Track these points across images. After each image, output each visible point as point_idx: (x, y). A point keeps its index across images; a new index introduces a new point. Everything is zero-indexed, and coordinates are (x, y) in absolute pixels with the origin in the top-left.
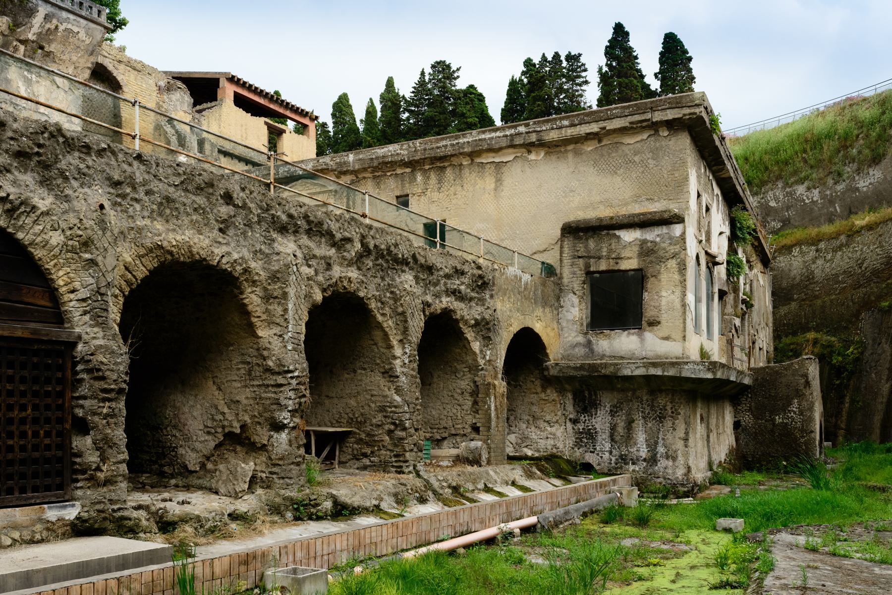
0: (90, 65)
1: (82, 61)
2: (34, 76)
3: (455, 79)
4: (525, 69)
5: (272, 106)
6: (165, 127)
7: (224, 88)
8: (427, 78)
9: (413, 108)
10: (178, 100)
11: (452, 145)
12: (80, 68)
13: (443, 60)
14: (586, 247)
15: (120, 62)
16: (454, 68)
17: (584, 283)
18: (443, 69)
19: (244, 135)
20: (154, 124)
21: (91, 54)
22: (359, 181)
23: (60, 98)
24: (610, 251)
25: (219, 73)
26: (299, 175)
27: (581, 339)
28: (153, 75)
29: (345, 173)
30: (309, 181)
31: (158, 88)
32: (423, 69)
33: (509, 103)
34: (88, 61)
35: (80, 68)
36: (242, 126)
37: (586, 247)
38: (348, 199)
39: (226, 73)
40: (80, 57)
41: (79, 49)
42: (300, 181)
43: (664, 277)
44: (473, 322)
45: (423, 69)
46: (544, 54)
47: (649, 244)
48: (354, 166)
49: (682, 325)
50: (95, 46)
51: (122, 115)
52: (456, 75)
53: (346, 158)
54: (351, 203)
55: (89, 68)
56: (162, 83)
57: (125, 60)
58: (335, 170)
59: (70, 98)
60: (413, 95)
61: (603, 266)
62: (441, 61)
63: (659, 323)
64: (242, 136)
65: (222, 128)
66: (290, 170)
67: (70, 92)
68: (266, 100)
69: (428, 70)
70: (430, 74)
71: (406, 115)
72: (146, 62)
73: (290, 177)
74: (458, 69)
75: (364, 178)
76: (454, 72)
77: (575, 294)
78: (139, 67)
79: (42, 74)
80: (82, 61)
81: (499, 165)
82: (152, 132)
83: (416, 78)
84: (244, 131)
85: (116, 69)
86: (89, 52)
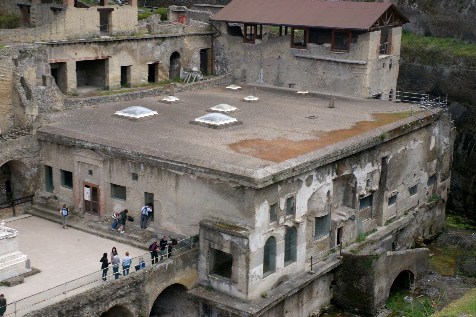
10: (27, 62)
11: (155, 161)
14: (209, 235)
17: (208, 252)
19: (83, 26)
24: (219, 241)
27: (206, 278)
36: (81, 19)
37: (209, 235)
43: (240, 262)
44: (131, 302)
47: (234, 244)
49: (246, 287)
61: (216, 247)
63: (237, 283)
77: (204, 256)
81: (177, 176)
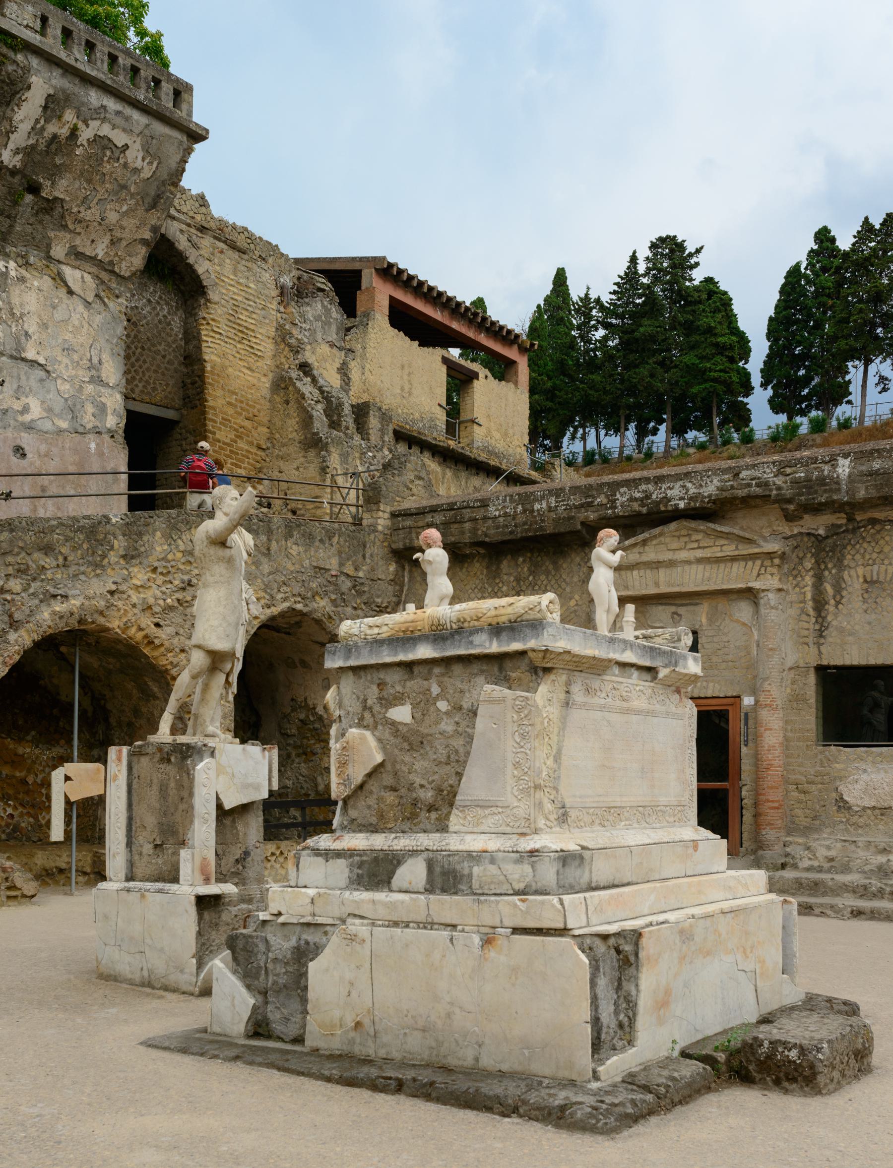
0: (147, 235)
1: (130, 223)
2: (12, 264)
3: (692, 267)
4: (816, 247)
5: (455, 325)
6: (298, 384)
7: (371, 290)
8: (642, 268)
9: (614, 321)
12: (124, 243)
13: (672, 234)
15: (202, 229)
16: (690, 248)
18: (672, 251)
20: (271, 375)
21: (154, 205)
22: (854, 531)
23: (75, 320)
25: (361, 259)
26: (676, 509)
28: (271, 260)
29: (816, 509)
30: (702, 525)
31: (278, 292)
32: (635, 252)
33: (785, 309)
34: (143, 223)
35: (124, 243)
36: (403, 367)
38: (819, 579)
39: (375, 258)
40: (125, 214)
41: (123, 194)
42: (673, 526)
45: (635, 252)
46: (867, 219)
48: (851, 491)
50: (163, 183)
51: (206, 357)
52: (692, 261)
53: (826, 469)
54: (829, 589)
55: (144, 242)
56: (287, 280)
57: (212, 225)
58: (789, 501)
59: (98, 319)
60: (614, 297)
62: (668, 237)
64: (402, 389)
65: (367, 373)
66: (648, 497)
67: (98, 305)
68: (446, 313)
69: (644, 253)
70: (647, 258)
71: (600, 333)
72: (257, 230)
73: (649, 514)
74: (698, 251)
75: (873, 522)
76: (691, 255)
78: (241, 242)
79: (32, 259)
80: (130, 223)
82: (268, 396)
83: (622, 267)
84: (406, 377)
85: (195, 246)
86: (148, 200)
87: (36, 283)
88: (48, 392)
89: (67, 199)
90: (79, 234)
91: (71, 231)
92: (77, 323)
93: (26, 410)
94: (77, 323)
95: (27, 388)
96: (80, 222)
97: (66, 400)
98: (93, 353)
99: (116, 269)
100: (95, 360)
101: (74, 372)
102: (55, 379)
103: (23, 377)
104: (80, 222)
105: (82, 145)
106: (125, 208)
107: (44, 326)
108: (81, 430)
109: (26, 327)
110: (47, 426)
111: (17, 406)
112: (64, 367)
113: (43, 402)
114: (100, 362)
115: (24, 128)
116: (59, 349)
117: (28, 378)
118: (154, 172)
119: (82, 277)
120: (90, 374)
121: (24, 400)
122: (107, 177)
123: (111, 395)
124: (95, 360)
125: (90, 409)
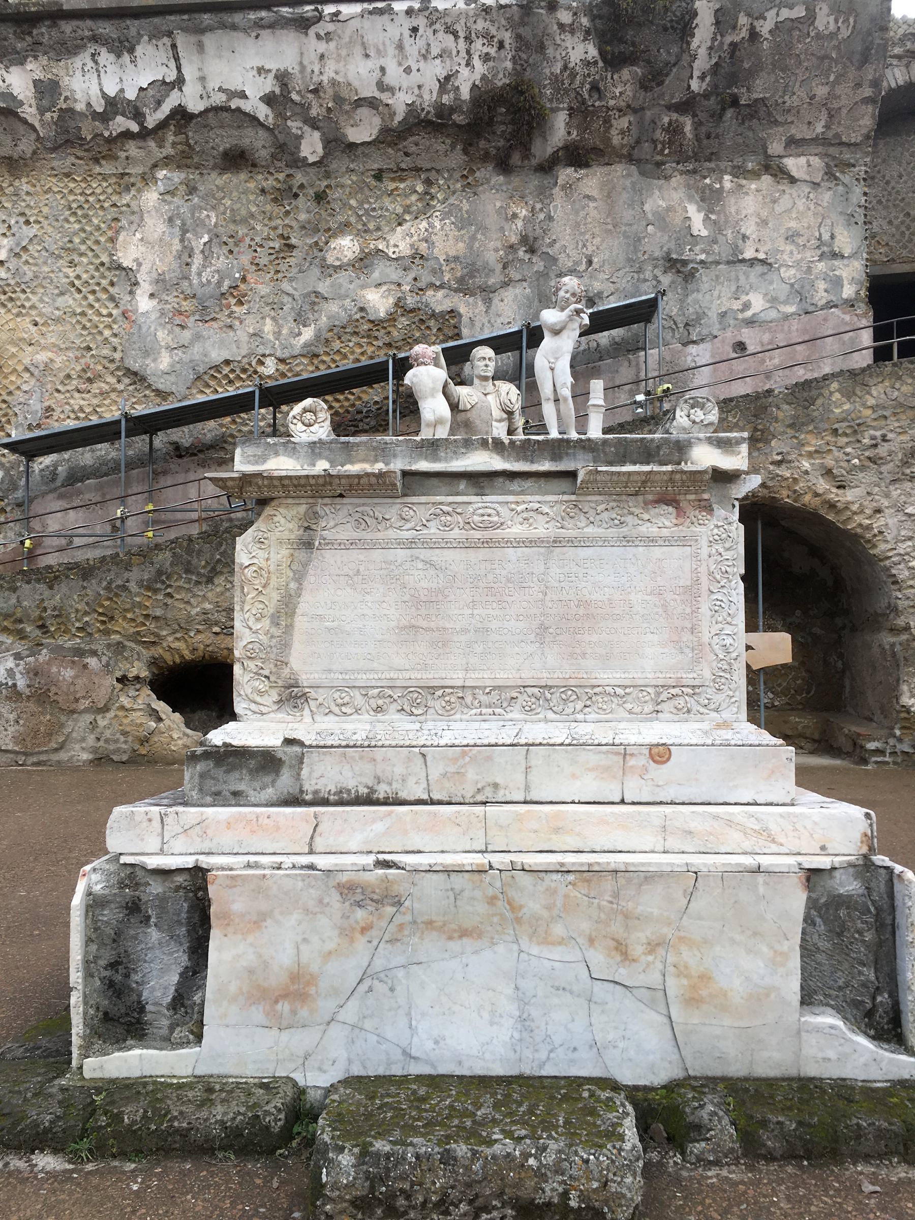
0: (868, 92)
35: (844, 111)
40: (837, 82)
55: (867, 101)
86: (857, 57)
87: (753, 186)
88: (771, 283)
89: (767, 95)
90: (792, 122)
91: (782, 124)
92: (801, 208)
93: (747, 306)
94: (801, 208)
95: (748, 287)
96: (789, 111)
97: (792, 285)
98: (822, 230)
99: (844, 139)
100: (826, 237)
101: (799, 256)
102: (778, 269)
103: (742, 278)
104: (789, 111)
105: (766, 39)
106: (832, 78)
107: (764, 223)
108: (811, 309)
109: (742, 231)
110: (773, 314)
111: (737, 305)
112: (788, 254)
113: (766, 295)
114: (832, 237)
115: (702, 52)
116: (782, 240)
117: (747, 277)
118: (854, 27)
119: (808, 161)
120: (819, 252)
121: (744, 298)
122: (802, 57)
123: (848, 266)
124: (826, 237)
125: (822, 285)
